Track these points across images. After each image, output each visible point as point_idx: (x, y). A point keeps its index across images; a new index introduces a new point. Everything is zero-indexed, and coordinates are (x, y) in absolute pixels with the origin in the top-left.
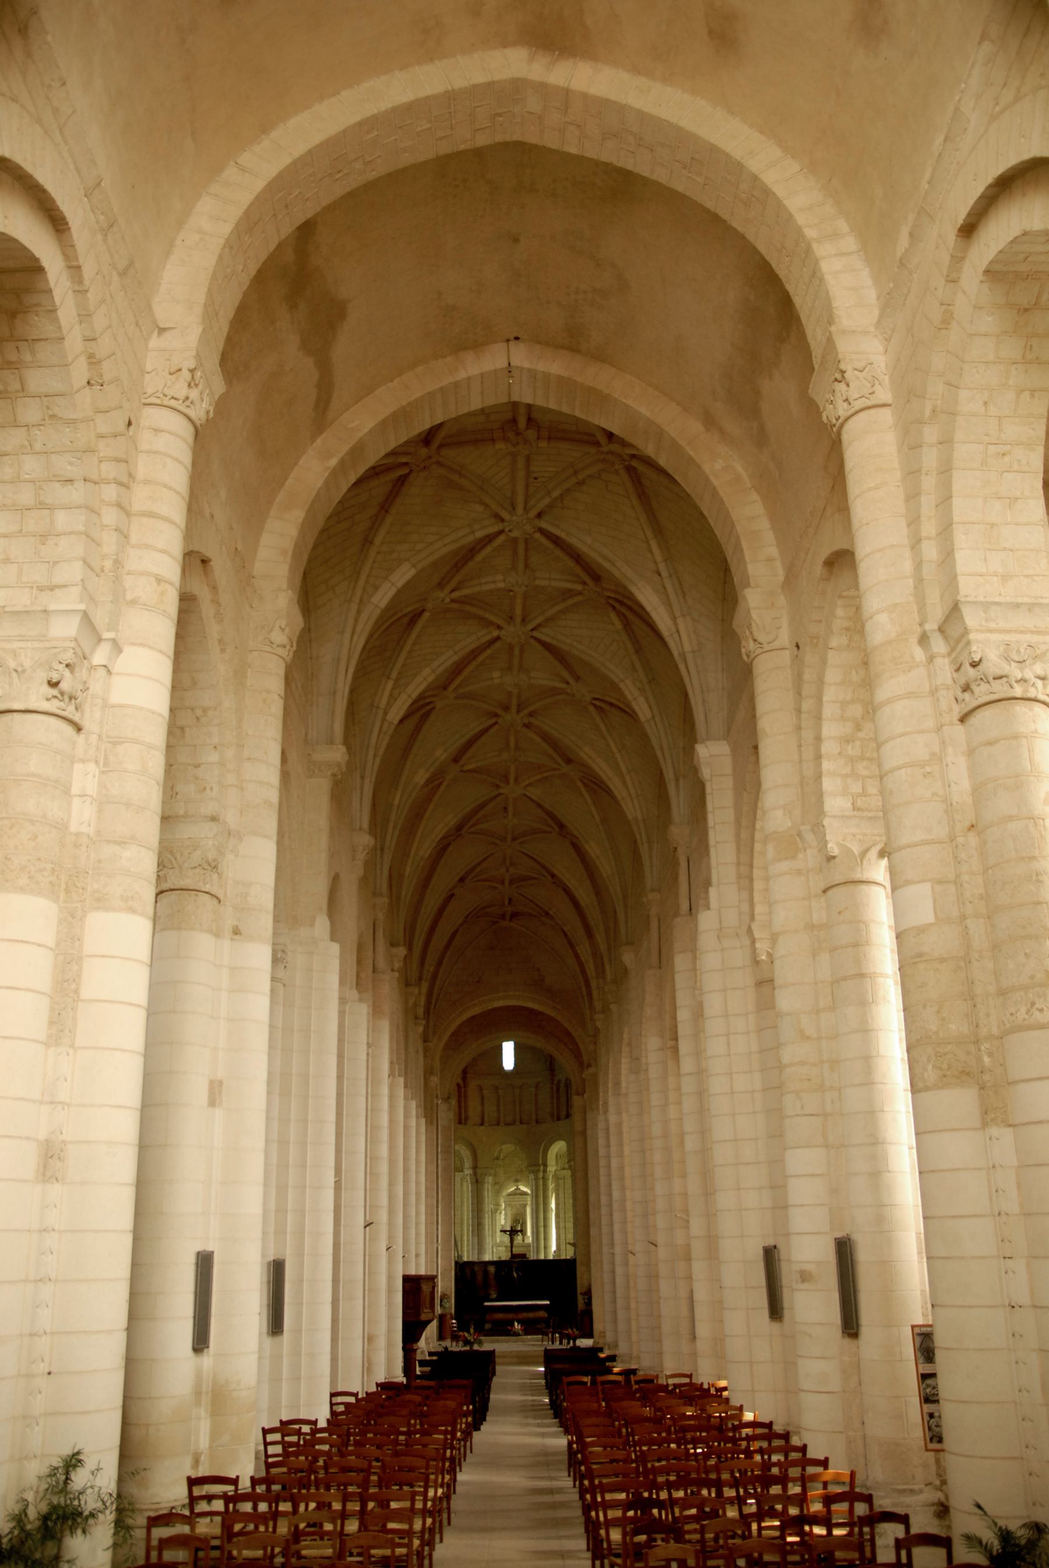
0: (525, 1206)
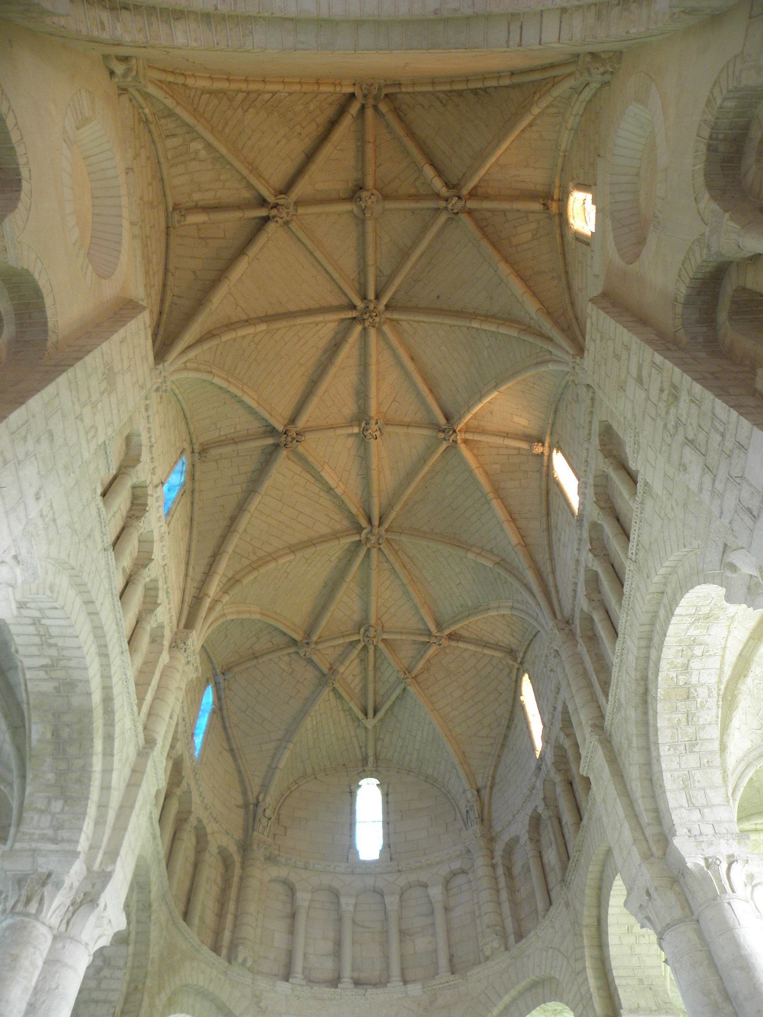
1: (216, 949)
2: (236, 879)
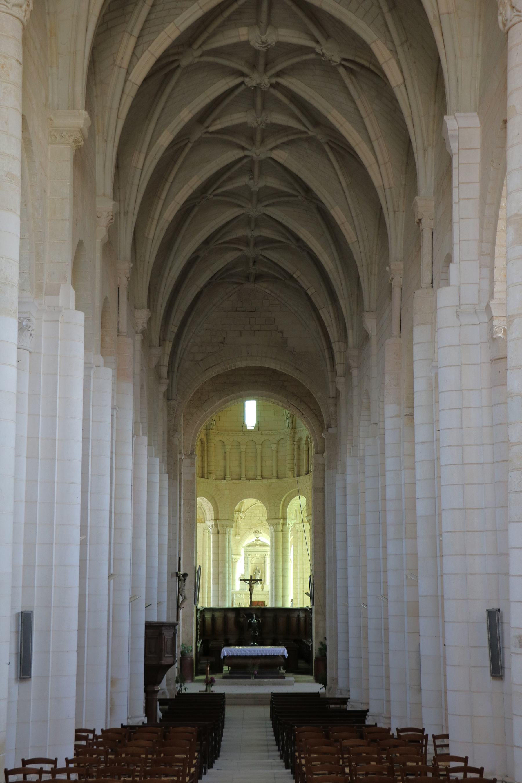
0: (264, 557)
2: (206, 448)
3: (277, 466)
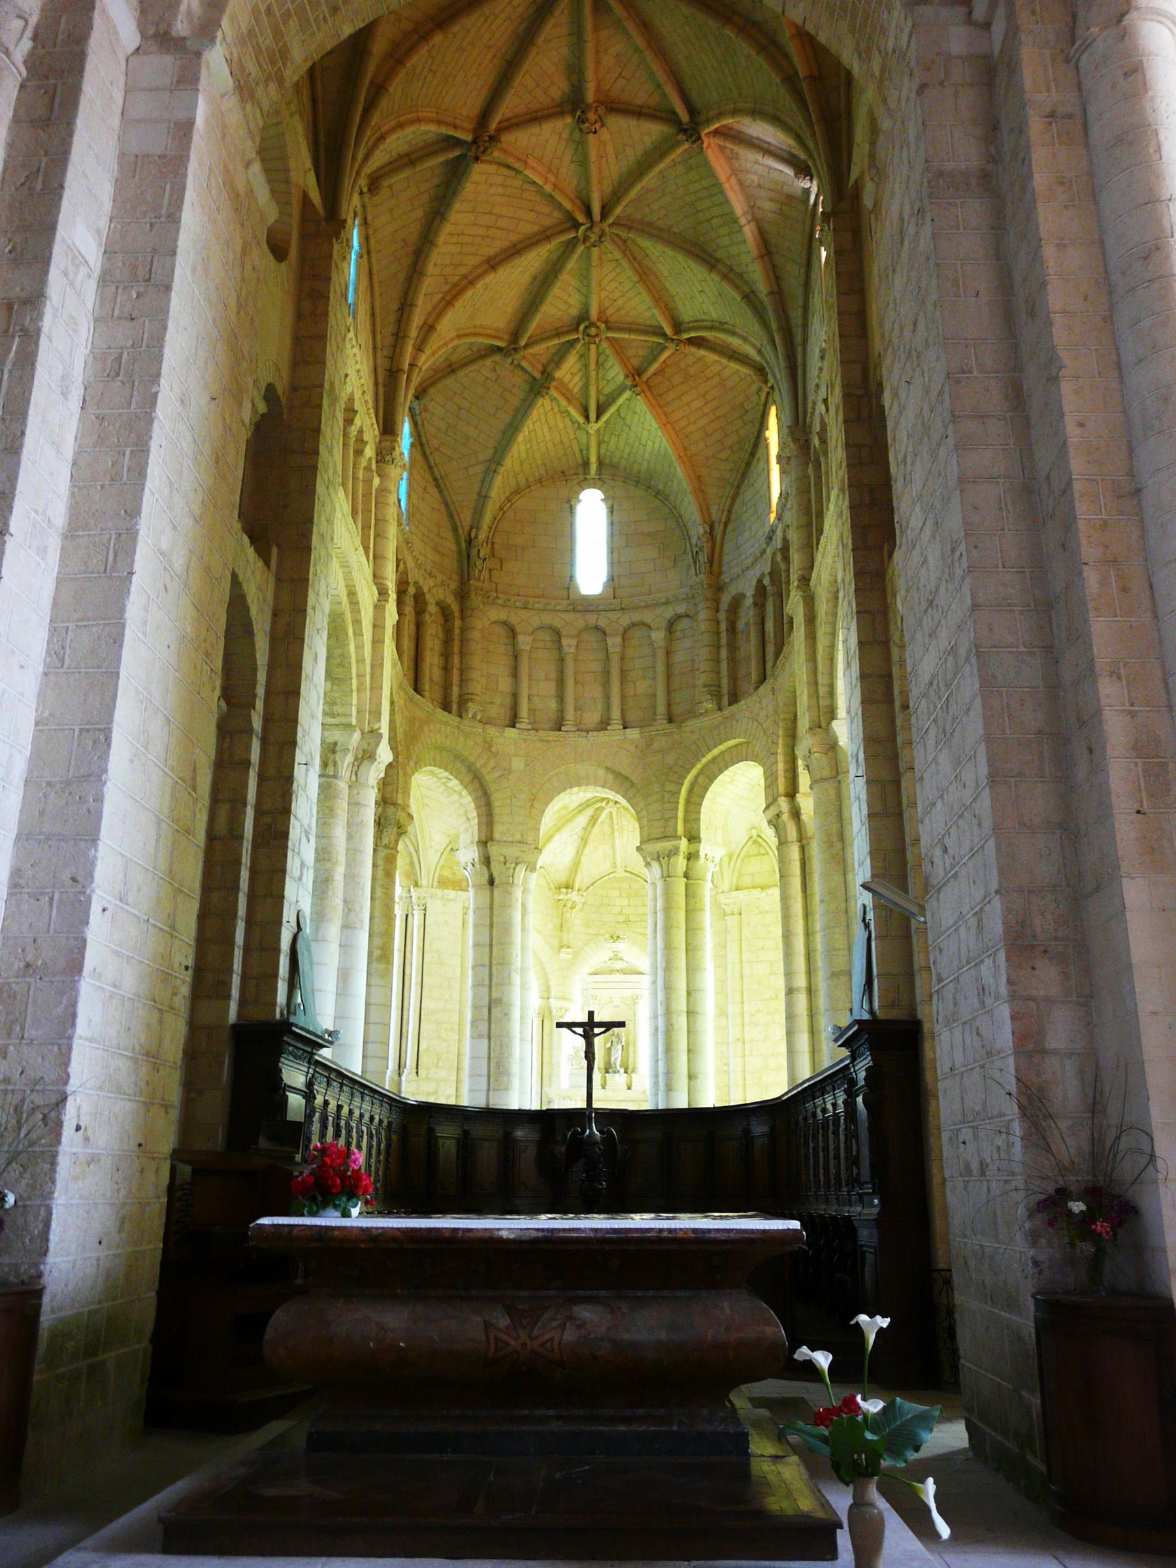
0: (635, 1000)
1: (446, 707)
2: (457, 631)
3: (669, 692)
